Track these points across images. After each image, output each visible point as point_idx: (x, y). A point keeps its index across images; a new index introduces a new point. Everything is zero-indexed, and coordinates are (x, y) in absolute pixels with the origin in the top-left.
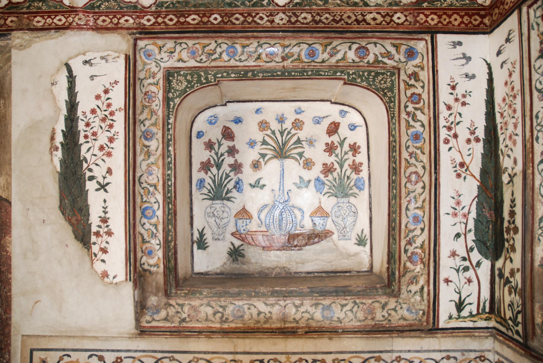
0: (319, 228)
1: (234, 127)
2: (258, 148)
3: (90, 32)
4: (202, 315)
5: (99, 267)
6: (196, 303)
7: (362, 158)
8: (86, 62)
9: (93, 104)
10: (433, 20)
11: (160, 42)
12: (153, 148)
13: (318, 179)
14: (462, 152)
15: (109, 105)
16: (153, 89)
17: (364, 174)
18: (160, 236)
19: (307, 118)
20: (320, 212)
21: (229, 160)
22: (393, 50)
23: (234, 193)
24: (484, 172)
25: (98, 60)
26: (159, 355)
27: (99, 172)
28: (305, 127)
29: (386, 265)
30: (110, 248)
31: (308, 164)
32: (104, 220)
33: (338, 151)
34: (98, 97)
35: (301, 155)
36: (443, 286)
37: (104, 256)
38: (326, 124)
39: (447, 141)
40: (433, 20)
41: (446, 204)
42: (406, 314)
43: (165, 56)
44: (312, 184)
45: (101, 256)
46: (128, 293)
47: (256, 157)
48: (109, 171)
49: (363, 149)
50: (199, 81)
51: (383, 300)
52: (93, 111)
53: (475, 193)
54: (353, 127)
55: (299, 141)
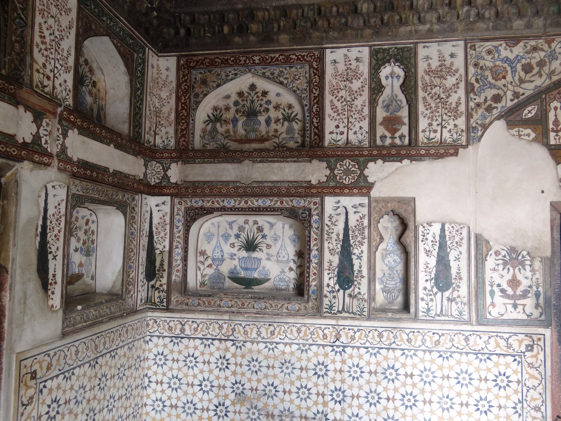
5: (50, 302)
8: (53, 187)
14: (144, 241)
17: (95, 245)
27: (53, 249)
35: (76, 234)
38: (85, 219)
54: (93, 222)
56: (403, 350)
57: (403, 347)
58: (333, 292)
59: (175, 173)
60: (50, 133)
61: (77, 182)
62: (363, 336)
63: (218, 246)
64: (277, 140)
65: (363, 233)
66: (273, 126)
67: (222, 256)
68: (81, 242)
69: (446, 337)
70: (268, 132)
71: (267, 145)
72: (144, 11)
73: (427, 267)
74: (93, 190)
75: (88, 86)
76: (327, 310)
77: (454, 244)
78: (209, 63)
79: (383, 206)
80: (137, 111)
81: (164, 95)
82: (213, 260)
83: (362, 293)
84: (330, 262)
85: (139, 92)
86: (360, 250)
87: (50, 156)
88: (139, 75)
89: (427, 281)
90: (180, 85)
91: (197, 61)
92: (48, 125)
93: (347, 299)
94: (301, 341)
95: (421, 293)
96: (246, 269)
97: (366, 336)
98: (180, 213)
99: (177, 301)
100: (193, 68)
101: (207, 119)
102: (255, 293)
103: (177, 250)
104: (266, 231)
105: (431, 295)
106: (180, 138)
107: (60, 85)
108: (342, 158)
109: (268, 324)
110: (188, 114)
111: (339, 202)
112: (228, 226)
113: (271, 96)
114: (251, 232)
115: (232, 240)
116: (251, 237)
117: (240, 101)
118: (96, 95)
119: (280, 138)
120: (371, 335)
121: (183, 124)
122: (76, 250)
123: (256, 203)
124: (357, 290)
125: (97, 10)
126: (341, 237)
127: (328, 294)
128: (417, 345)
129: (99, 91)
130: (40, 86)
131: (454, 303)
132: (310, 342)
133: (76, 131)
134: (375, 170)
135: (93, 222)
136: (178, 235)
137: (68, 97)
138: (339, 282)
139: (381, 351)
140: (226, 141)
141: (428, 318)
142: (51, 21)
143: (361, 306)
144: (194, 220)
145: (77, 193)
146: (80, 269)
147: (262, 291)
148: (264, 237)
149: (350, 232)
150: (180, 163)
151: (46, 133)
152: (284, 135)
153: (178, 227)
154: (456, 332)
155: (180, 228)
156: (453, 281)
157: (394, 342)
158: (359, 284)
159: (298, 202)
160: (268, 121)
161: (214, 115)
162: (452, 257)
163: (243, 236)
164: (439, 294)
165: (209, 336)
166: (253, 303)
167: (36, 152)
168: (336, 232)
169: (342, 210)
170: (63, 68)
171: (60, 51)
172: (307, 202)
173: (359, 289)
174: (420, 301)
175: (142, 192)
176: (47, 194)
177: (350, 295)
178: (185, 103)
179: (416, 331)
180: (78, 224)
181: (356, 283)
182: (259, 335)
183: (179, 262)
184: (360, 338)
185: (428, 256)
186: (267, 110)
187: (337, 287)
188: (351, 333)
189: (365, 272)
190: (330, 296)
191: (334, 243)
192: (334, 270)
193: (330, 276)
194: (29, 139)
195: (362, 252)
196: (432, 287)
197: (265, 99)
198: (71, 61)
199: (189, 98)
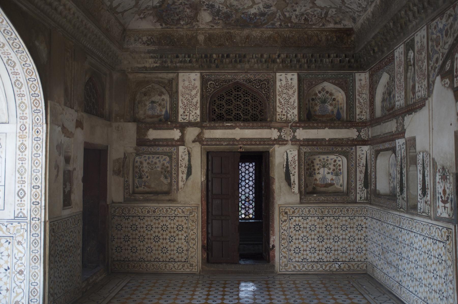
5: (293, 191)
7: (341, 167)
9: (292, 159)
10: (356, 143)
17: (342, 171)
19: (329, 158)
27: (293, 172)
31: (330, 169)
32: (294, 181)
38: (333, 160)
46: (298, 195)
54: (339, 161)
60: (286, 133)
72: (339, 62)
74: (317, 149)
75: (329, 102)
80: (351, 106)
87: (287, 141)
92: (284, 131)
122: (328, 173)
129: (338, 101)
133: (301, 129)
175: (356, 145)
176: (287, 154)
180: (328, 162)
194: (276, 137)
198: (296, 104)
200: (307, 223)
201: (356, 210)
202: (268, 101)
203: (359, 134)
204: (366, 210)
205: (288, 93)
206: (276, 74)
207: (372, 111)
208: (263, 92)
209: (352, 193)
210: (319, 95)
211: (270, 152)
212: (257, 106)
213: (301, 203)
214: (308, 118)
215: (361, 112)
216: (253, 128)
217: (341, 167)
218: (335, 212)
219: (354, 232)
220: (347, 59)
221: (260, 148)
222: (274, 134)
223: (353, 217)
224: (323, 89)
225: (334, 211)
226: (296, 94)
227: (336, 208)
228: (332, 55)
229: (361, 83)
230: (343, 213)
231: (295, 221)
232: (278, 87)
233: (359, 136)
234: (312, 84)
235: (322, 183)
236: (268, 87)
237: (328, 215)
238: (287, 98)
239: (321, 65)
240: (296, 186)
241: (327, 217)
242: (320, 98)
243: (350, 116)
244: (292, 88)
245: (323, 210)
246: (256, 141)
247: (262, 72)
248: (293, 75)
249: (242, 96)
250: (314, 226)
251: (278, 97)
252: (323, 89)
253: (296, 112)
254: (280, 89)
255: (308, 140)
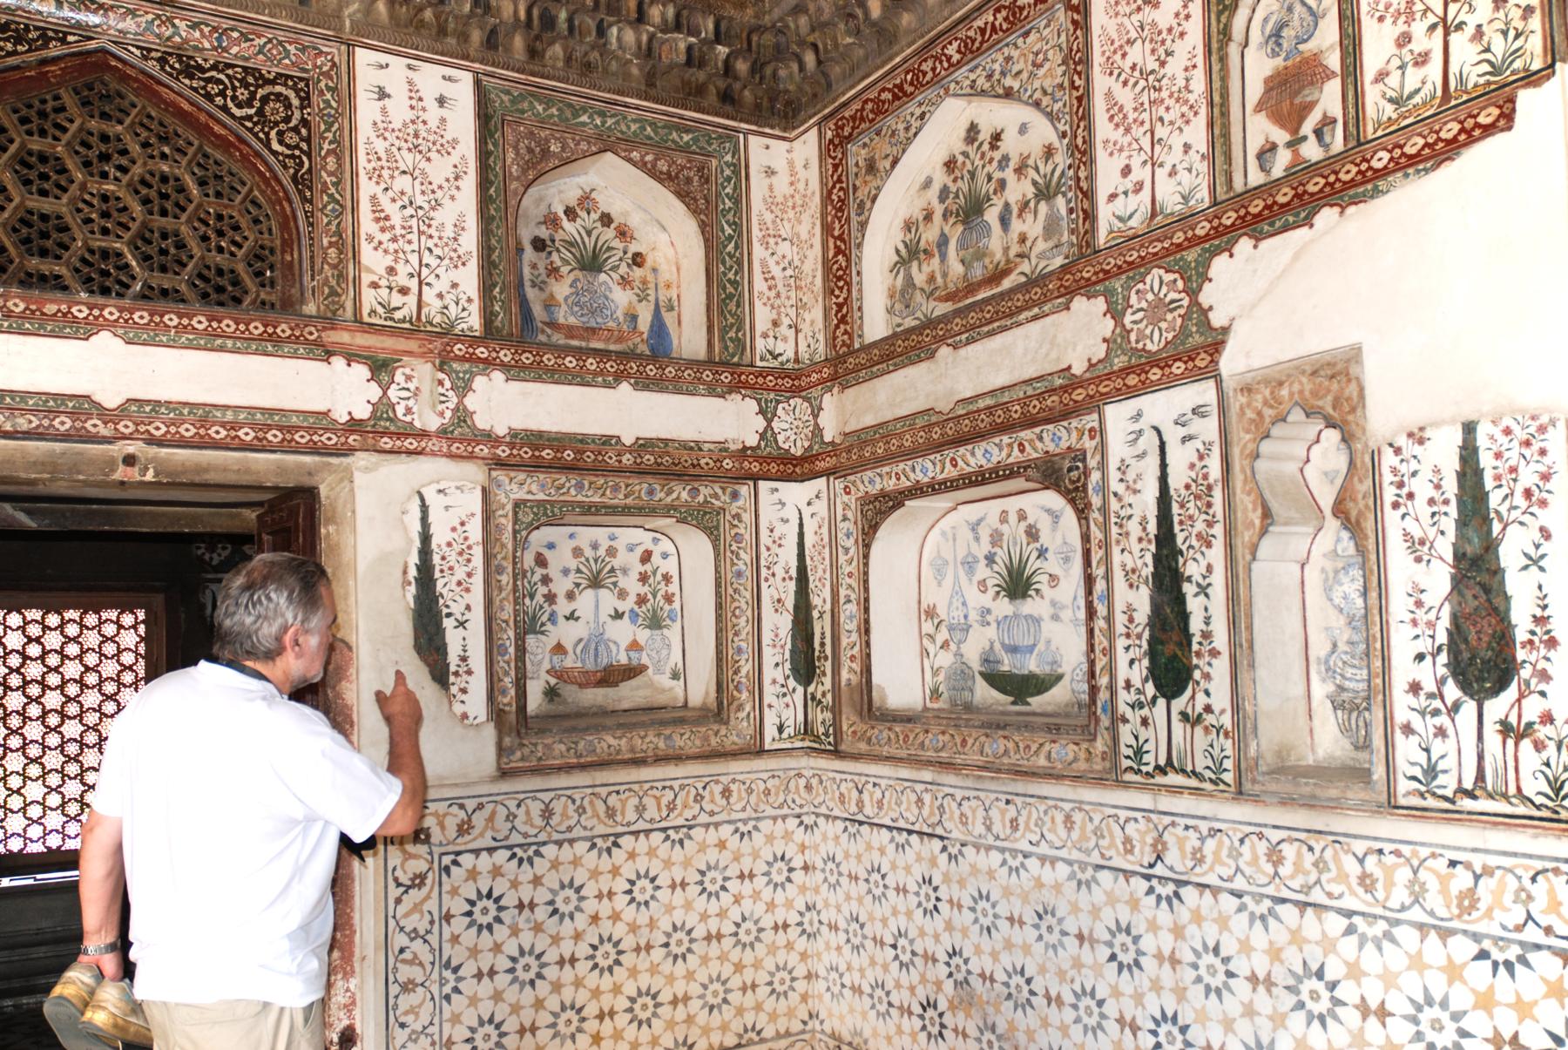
0: (635, 662)
1: (547, 553)
2: (572, 575)
3: (444, 460)
4: (557, 752)
5: (458, 709)
6: (548, 741)
7: (674, 588)
9: (449, 536)
10: (755, 467)
11: (513, 474)
12: (504, 582)
13: (632, 611)
14: (779, 590)
15: (466, 539)
16: (503, 520)
17: (676, 605)
18: (513, 673)
19: (620, 545)
20: (635, 646)
21: (543, 590)
22: (719, 492)
23: (549, 626)
24: (796, 607)
25: (453, 490)
26: (522, 796)
27: (457, 609)
28: (619, 554)
29: (713, 694)
30: (470, 688)
31: (622, 595)
32: (464, 659)
33: (651, 580)
34: (454, 529)
35: (615, 584)
36: (766, 710)
37: (464, 697)
38: (639, 551)
39: (767, 580)
40: (755, 467)
41: (767, 638)
42: (735, 739)
43: (514, 487)
44: (626, 616)
45: (461, 697)
46: (490, 732)
47: (570, 586)
48: (468, 608)
49: (676, 579)
50: (545, 514)
51: (715, 727)
52: (449, 544)
53: (790, 626)
54: (665, 556)
55: (612, 570)
56: (1349, 914)
57: (1349, 903)
58: (1141, 706)
59: (839, 414)
61: (522, 476)
62: (1225, 852)
63: (957, 591)
64: (1025, 267)
65: (1209, 505)
66: (1017, 226)
67: (966, 617)
68: (632, 599)
69: (1502, 884)
70: (1006, 249)
71: (1007, 283)
72: (682, 58)
73: (1419, 604)
74: (579, 486)
75: (615, 268)
76: (1128, 763)
77: (1519, 499)
78: (872, 111)
79: (1266, 403)
80: (730, 289)
81: (803, 230)
82: (951, 629)
83: (1216, 708)
84: (1130, 611)
85: (730, 248)
86: (1203, 564)
87: (423, 434)
88: (729, 204)
89: (1420, 657)
90: (830, 193)
91: (853, 118)
92: (409, 378)
93: (1178, 727)
94: (1076, 855)
95: (1403, 707)
96: (1013, 650)
97: (1235, 854)
98: (850, 515)
99: (854, 732)
100: (849, 138)
101: (896, 258)
102: (1034, 714)
103: (848, 606)
104: (1045, 539)
105: (1436, 713)
106: (837, 327)
107: (440, 296)
108: (1135, 269)
109: (1004, 797)
110: (848, 260)
111: (1138, 416)
112: (970, 535)
113: (1011, 145)
114: (1015, 544)
115: (982, 571)
116: (1016, 561)
117: (950, 184)
118: (644, 282)
119: (1033, 256)
120: (1246, 849)
121: (841, 289)
122: (618, 615)
123: (972, 461)
124: (1201, 700)
125: (554, 111)
126: (1152, 528)
127: (1129, 713)
128: (1394, 903)
129: (654, 270)
130: (380, 310)
131: (1526, 744)
132: (1096, 858)
133: (498, 376)
134: (1239, 282)
135: (665, 556)
136: (847, 569)
137: (465, 314)
138: (1154, 673)
139: (1280, 908)
140: (932, 304)
141: (1431, 802)
142: (403, 183)
143: (1216, 752)
144: (874, 527)
145: (530, 497)
146: (632, 654)
147: (1049, 709)
148: (1042, 553)
149: (1175, 509)
150: (836, 390)
151: (405, 394)
152: (1041, 245)
153: (847, 550)
154: (1539, 865)
155: (852, 551)
156: (1521, 655)
157: (1318, 882)
158: (1207, 676)
159: (1056, 439)
160: (1004, 221)
161: (906, 246)
162: (1510, 555)
163: (1001, 556)
164: (1470, 707)
165: (902, 824)
166: (983, 739)
167: (383, 434)
168: (1137, 513)
169: (1149, 442)
170: (446, 261)
171: (432, 231)
172: (1074, 434)
173: (1207, 693)
174: (1399, 737)
175: (755, 478)
176: (424, 508)
177: (1185, 716)
178: (840, 238)
179: (1387, 847)
180: (616, 563)
181: (1197, 675)
182: (989, 829)
183: (855, 637)
184: (1217, 859)
185: (1418, 560)
186: (1002, 184)
187: (1150, 689)
188: (1193, 840)
189: (1221, 640)
190: (1134, 717)
191: (1136, 548)
192: (1139, 637)
193: (1131, 654)
194: (363, 412)
195: (1209, 568)
196: (1441, 682)
197: (997, 155)
198: (470, 241)
199: (848, 220)
200: (537, 881)
201: (762, 786)
202: (305, 200)
203: (769, 426)
204: (802, 782)
205: (423, 172)
206: (350, 56)
207: (842, 312)
208: (276, 146)
209: (740, 708)
210: (566, 223)
211: (323, 491)
212: (236, 228)
213: (504, 774)
214: (516, 332)
215: (775, 324)
216: (211, 342)
217: (674, 588)
218: (671, 807)
219: (756, 895)
220: (723, 50)
221: (267, 466)
222: (342, 389)
223: (750, 826)
224: (586, 200)
225: (664, 801)
226: (470, 183)
227: (676, 784)
228: (655, 13)
229: (771, 188)
230: (708, 807)
231: (473, 874)
232: (364, 131)
233: (767, 434)
234: (546, 152)
235: (590, 666)
236: (305, 122)
237: (641, 825)
238: (420, 200)
239: (594, 56)
240: (478, 685)
241: (636, 833)
242: (571, 244)
243: (722, 339)
244: (444, 151)
245: (613, 800)
246: (233, 426)
247: (267, 26)
248: (449, 79)
249: (135, 149)
250: (570, 892)
251: (367, 188)
252: (586, 200)
253: (469, 279)
254: (380, 146)
255: (536, 439)
